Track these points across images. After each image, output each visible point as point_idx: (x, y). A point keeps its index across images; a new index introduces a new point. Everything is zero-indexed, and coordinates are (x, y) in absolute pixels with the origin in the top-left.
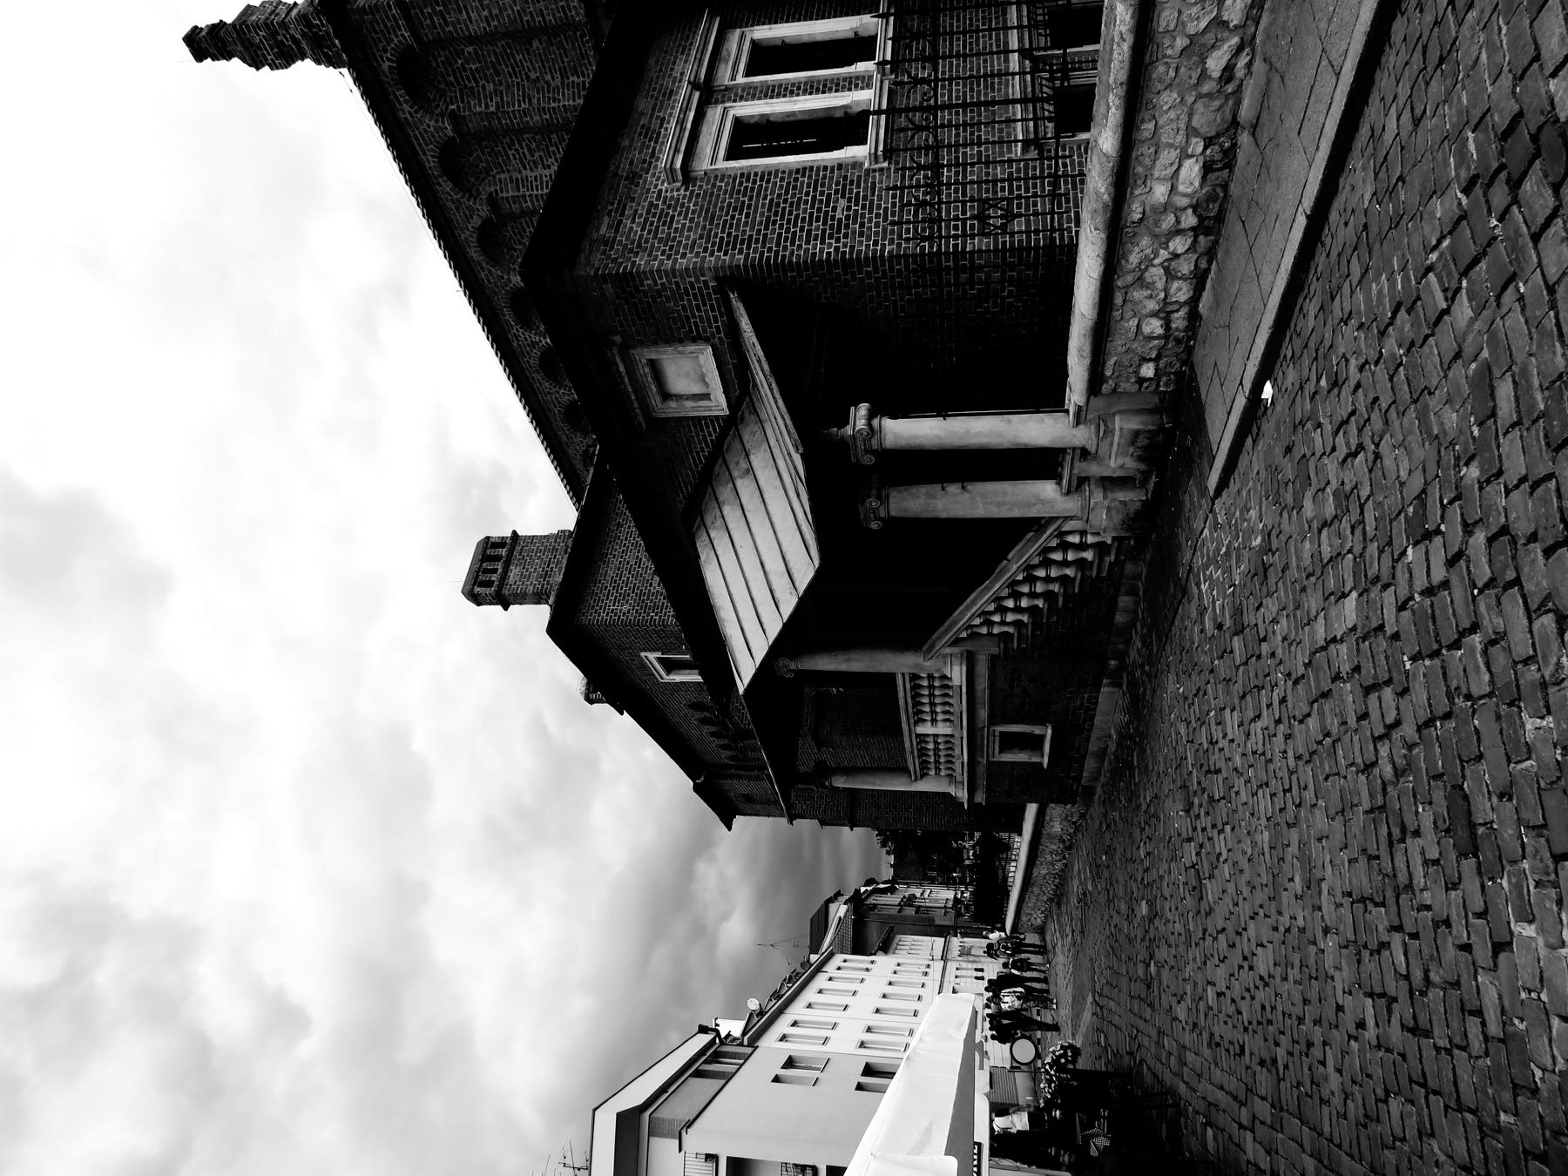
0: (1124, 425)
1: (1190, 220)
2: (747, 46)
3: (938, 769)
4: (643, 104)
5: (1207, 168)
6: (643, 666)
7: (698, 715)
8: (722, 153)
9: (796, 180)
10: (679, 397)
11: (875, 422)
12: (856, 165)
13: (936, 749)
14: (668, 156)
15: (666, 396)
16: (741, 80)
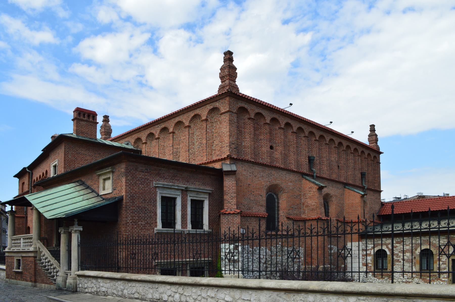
2: (203, 199)
8: (164, 195)
9: (153, 213)
11: (78, 232)
14: (162, 183)
16: (189, 199)
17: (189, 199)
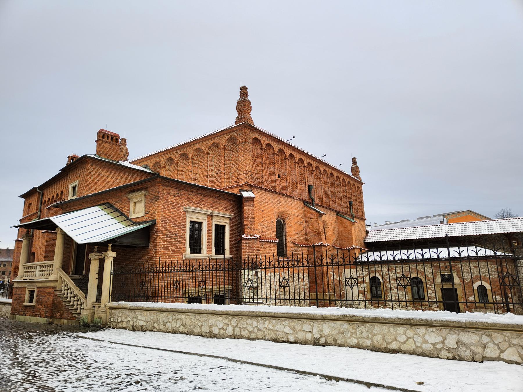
0: (103, 316)
1: (135, 324)
3: (26, 272)
4: (210, 200)
5: (142, 326)
6: (74, 180)
7: (59, 194)
8: (192, 220)
10: (135, 206)
12: (185, 251)
13: (32, 272)
15: (135, 203)
16: (214, 223)
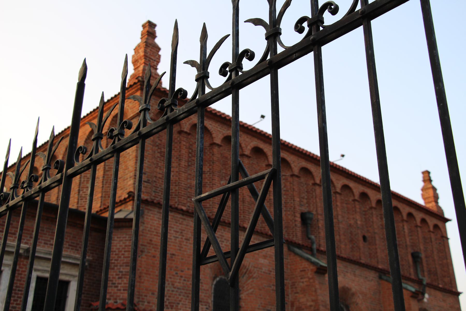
17: (34, 275)
